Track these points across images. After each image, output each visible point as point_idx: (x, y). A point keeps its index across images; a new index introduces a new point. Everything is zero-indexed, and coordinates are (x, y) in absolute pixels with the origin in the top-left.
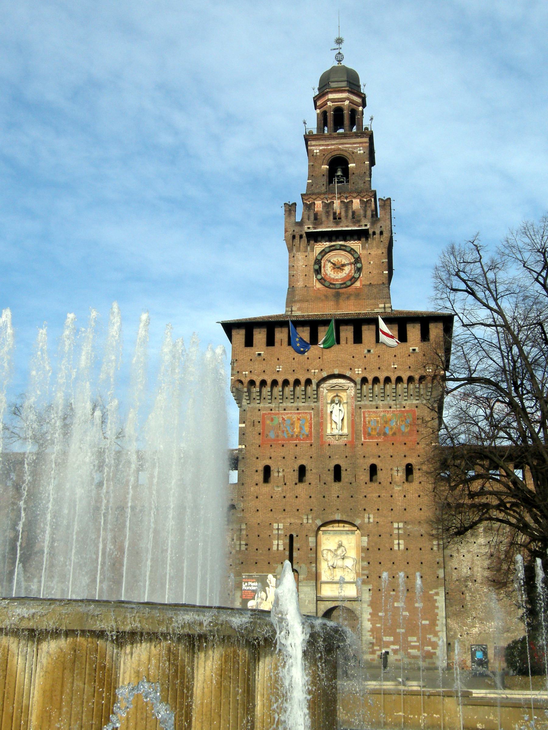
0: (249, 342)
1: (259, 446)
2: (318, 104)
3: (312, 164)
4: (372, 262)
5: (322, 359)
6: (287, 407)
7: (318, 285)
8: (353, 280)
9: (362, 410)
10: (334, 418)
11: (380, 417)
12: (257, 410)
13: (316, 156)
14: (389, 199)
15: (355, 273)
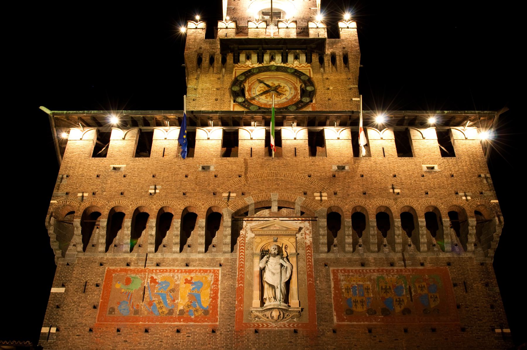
1: (91, 330)
4: (331, 88)
5: (246, 178)
6: (163, 260)
9: (331, 269)
10: (268, 277)
11: (370, 280)
12: (97, 264)
15: (302, 96)
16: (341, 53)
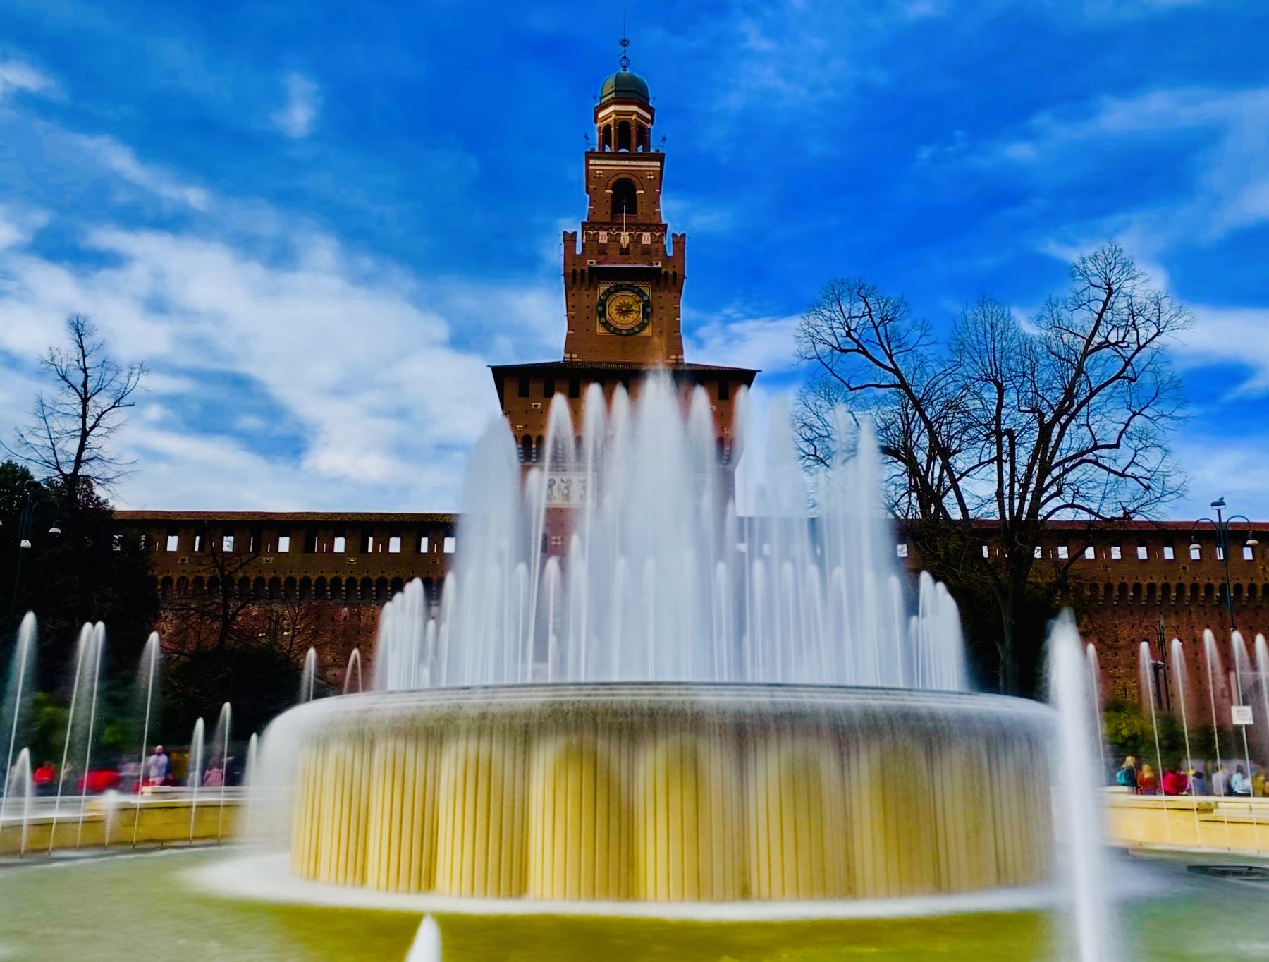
0: (524, 392)
2: (601, 115)
3: (594, 187)
7: (601, 331)
8: (642, 326)
13: (600, 178)
14: (683, 235)
16: (671, 273)
